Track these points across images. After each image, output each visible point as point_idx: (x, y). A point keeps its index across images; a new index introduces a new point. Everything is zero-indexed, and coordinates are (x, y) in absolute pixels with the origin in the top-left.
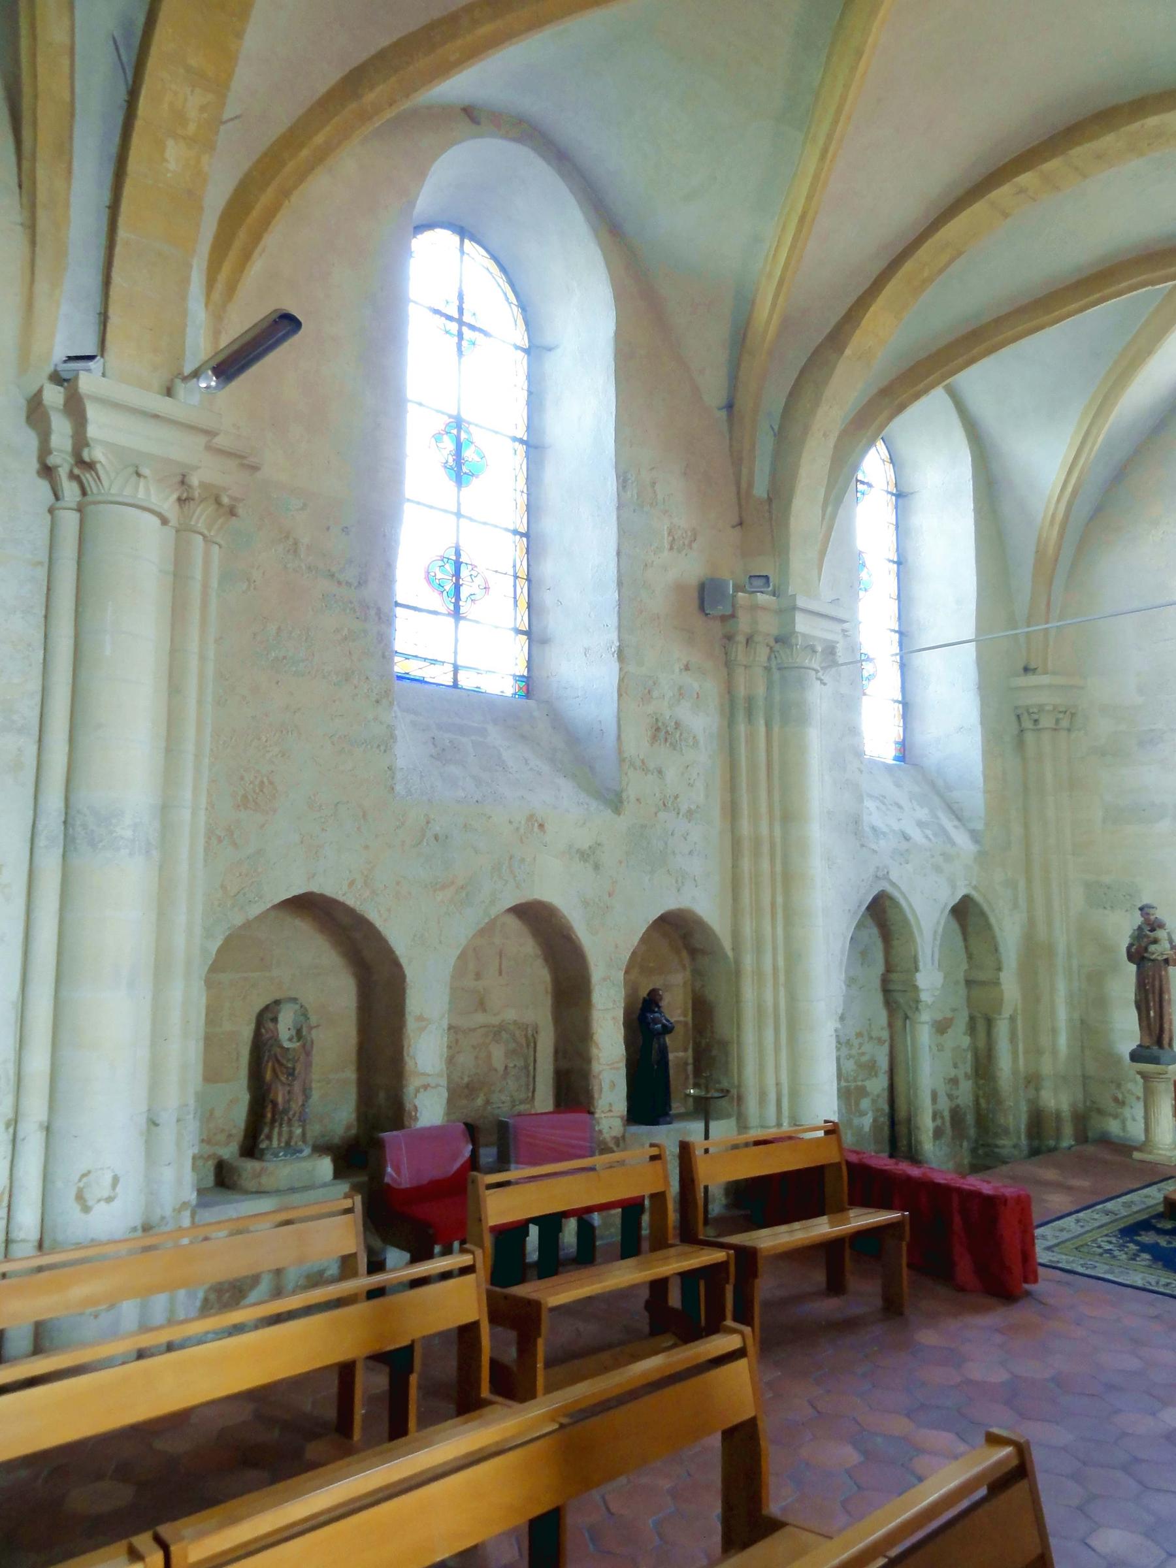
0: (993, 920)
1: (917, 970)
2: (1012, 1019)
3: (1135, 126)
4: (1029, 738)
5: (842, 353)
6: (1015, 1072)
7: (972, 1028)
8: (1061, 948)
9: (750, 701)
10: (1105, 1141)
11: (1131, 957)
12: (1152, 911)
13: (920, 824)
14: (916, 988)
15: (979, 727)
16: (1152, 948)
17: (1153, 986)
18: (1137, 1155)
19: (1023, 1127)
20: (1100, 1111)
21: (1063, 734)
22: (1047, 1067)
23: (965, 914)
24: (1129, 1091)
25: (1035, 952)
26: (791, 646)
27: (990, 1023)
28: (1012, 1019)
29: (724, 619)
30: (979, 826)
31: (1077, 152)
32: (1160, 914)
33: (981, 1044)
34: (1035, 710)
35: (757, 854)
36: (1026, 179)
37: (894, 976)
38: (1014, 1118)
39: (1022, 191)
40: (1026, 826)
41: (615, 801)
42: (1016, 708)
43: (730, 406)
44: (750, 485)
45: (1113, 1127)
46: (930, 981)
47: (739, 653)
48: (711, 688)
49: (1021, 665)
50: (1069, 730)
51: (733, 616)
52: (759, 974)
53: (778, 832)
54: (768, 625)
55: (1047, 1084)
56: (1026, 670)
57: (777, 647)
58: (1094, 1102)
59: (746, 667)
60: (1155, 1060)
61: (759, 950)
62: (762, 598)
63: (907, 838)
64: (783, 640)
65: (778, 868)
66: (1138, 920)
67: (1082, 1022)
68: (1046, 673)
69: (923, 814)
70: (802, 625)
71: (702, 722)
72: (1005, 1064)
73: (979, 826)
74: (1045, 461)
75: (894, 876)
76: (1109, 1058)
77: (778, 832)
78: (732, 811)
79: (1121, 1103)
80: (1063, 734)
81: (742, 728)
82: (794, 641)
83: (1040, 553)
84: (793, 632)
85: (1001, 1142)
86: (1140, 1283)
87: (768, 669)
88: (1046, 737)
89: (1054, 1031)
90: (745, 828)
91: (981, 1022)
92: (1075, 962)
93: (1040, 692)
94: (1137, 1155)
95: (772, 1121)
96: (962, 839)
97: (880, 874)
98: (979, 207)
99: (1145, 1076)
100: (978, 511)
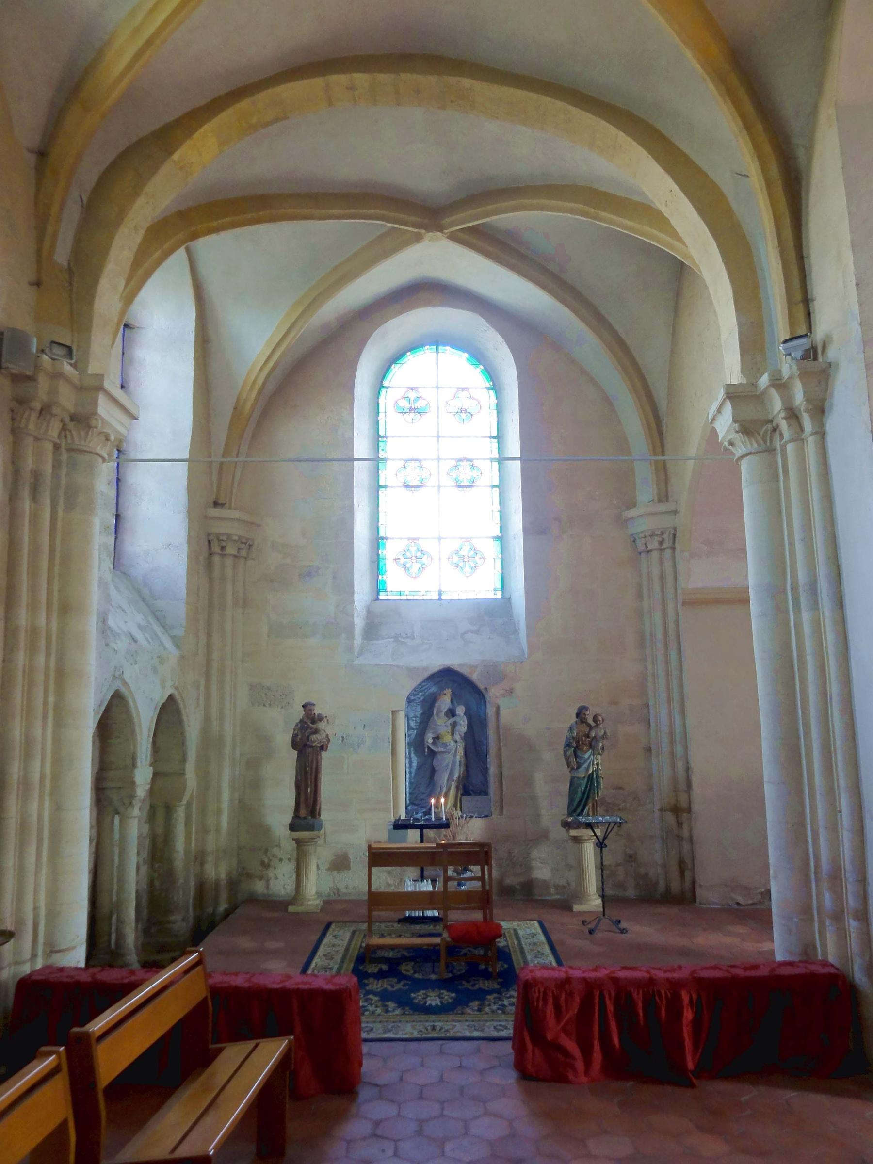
0: (184, 717)
1: (134, 766)
2: (189, 805)
3: (453, 80)
4: (216, 559)
5: (170, 153)
6: (187, 852)
8: (229, 740)
9: (37, 475)
10: (253, 900)
11: (294, 744)
12: (312, 707)
13: (140, 627)
14: (133, 783)
15: (186, 547)
16: (313, 737)
17: (312, 768)
18: (291, 909)
19: (191, 900)
20: (249, 876)
21: (242, 561)
22: (211, 844)
23: (169, 712)
24: (274, 856)
25: (211, 742)
26: (89, 427)
27: (169, 810)
28: (189, 805)
29: (17, 379)
30: (180, 632)
31: (408, 78)
32: (317, 711)
33: (160, 830)
34: (224, 538)
35: (32, 649)
36: (361, 78)
37: (111, 774)
38: (184, 894)
39: (351, 88)
40: (209, 635)
42: (209, 534)
43: (42, 154)
44: (53, 247)
45: (259, 887)
46: (143, 776)
47: (32, 424)
49: (212, 500)
50: (246, 558)
51: (31, 379)
52: (25, 784)
53: (54, 625)
54: (67, 399)
55: (210, 859)
56: (216, 504)
57: (71, 425)
58: (244, 868)
59: (37, 439)
60: (311, 828)
61: (28, 755)
62: (67, 368)
63: (135, 640)
64: (83, 420)
65: (52, 665)
66: (299, 713)
67: (240, 801)
68: (230, 508)
69: (139, 618)
70: (104, 408)
72: (180, 844)
73: (180, 632)
74: (255, 338)
75: (126, 676)
76: (260, 830)
77: (54, 625)
79: (266, 866)
80: (242, 561)
81: (26, 505)
82: (93, 423)
83: (237, 409)
84: (95, 413)
85: (173, 918)
86: (416, 1034)
87: (57, 447)
88: (229, 561)
89: (219, 812)
90: (23, 618)
91: (161, 808)
92: (238, 752)
93: (228, 523)
94: (291, 909)
95: (27, 955)
97: (117, 674)
98: (318, 82)
99: (299, 842)
100: (196, 359)
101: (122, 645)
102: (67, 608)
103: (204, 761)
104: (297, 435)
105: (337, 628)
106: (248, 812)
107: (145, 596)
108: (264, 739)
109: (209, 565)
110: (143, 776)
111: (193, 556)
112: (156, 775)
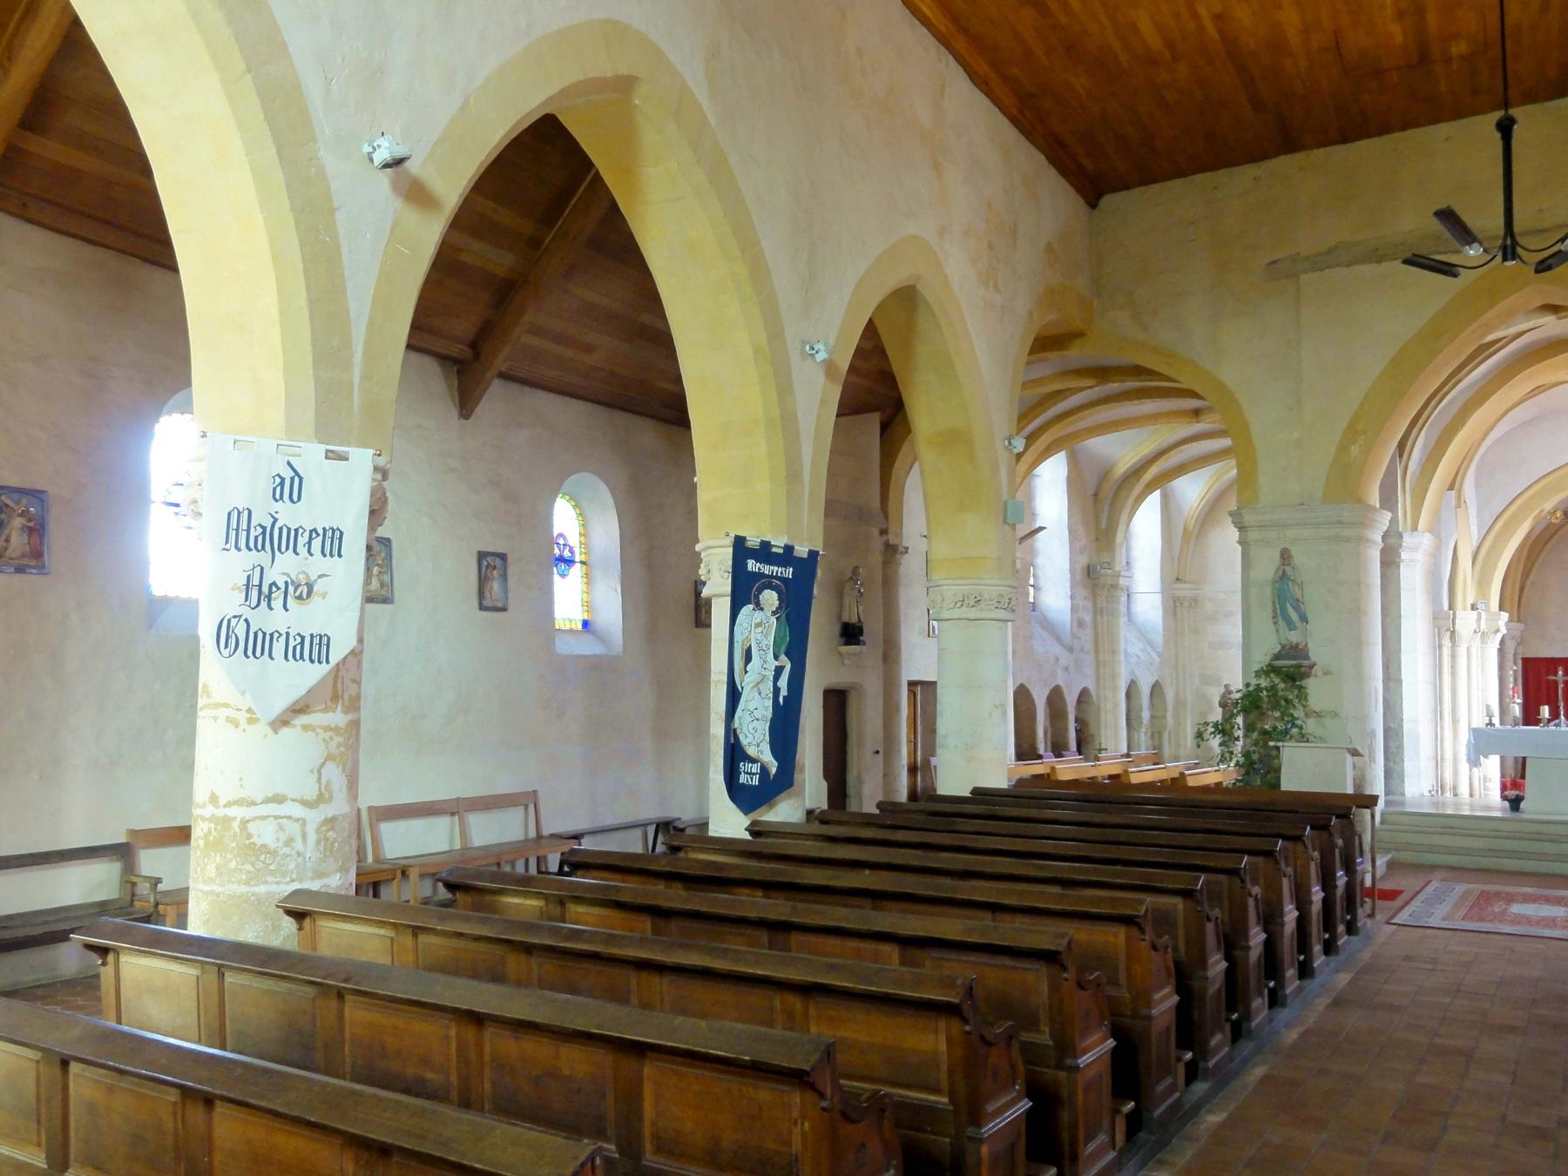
7: (1152, 737)
11: (1221, 705)
23: (1156, 689)
27: (1160, 733)
41: (1071, 650)
43: (1096, 495)
46: (1146, 715)
48: (1089, 604)
64: (1115, 586)
66: (1223, 690)
69: (1141, 646)
71: (1088, 618)
78: (1097, 650)
93: (1184, 590)
96: (1155, 656)
101: (1134, 660)
102: (1114, 653)
107: (1143, 635)
109: (1175, 614)
110: (1146, 715)
111: (1165, 609)
112: (1152, 717)
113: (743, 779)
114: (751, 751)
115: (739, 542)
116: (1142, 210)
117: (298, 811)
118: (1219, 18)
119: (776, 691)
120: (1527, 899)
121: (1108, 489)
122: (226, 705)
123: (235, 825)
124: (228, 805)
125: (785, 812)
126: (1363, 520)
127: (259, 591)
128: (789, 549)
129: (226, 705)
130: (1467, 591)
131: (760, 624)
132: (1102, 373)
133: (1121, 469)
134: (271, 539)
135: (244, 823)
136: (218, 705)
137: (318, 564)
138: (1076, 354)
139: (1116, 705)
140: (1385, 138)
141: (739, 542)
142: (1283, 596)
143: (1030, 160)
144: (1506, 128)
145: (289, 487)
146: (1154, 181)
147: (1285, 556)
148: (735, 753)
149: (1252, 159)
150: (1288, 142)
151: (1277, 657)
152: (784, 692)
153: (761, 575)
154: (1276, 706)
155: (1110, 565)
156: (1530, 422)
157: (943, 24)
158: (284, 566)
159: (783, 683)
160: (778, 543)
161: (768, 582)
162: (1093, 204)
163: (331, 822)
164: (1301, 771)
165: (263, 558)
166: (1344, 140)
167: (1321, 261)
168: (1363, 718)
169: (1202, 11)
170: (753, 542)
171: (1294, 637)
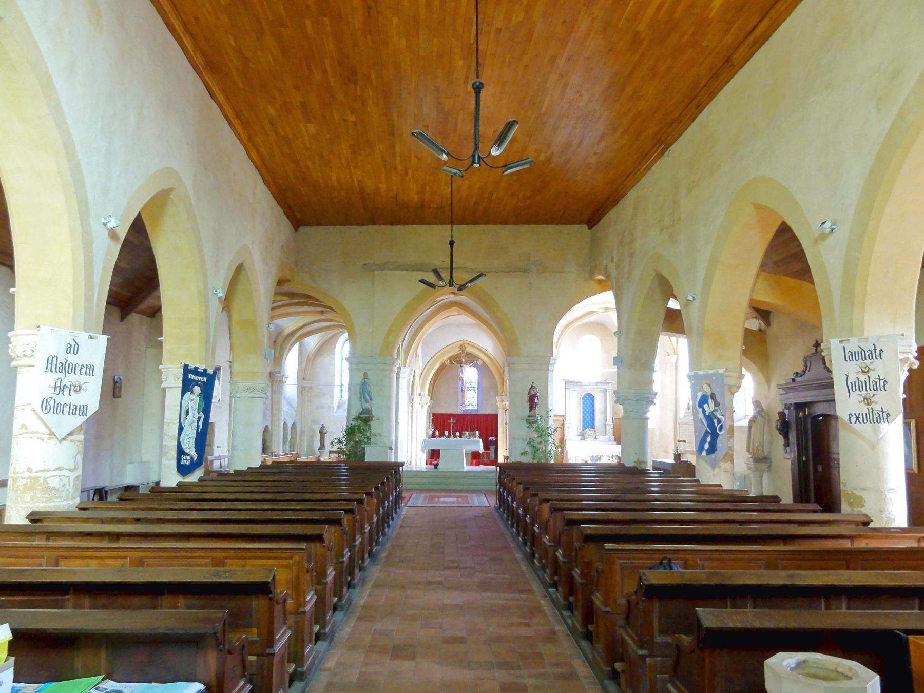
23: (294, 425)
25: (302, 432)
46: (289, 437)
78: (272, 409)
93: (306, 383)
102: (279, 410)
103: (301, 436)
104: (324, 360)
105: (331, 407)
106: (310, 447)
108: (314, 431)
110: (289, 437)
113: (183, 462)
114: (187, 451)
115: (186, 366)
116: (314, 234)
117: (67, 473)
118: (360, 181)
119: (198, 427)
120: (444, 497)
121: (281, 339)
122: (37, 432)
123: (41, 480)
124: (38, 472)
125: (195, 477)
126: (392, 364)
127: (59, 388)
128: (205, 370)
129: (37, 432)
130: (418, 389)
131: (193, 399)
132: (292, 295)
133: (287, 331)
134: (66, 368)
135: (45, 479)
136: (32, 433)
137: (83, 378)
138: (285, 288)
139: (279, 432)
140: (406, 226)
141: (186, 366)
142: (363, 389)
143: (279, 212)
144: (452, 243)
145: (73, 348)
146: (321, 224)
147: (365, 375)
148: (181, 452)
149: (358, 224)
150: (373, 222)
151: (361, 413)
152: (201, 427)
153: (193, 380)
154: (360, 432)
155: (279, 372)
156: (442, 327)
157: (259, 163)
158: (70, 379)
159: (201, 424)
160: (201, 368)
161: (197, 383)
162: (296, 230)
163: (77, 477)
164: (372, 455)
165: (62, 375)
166: (392, 224)
167: (383, 267)
168: (389, 436)
169: (355, 178)
170: (191, 367)
171: (367, 406)
